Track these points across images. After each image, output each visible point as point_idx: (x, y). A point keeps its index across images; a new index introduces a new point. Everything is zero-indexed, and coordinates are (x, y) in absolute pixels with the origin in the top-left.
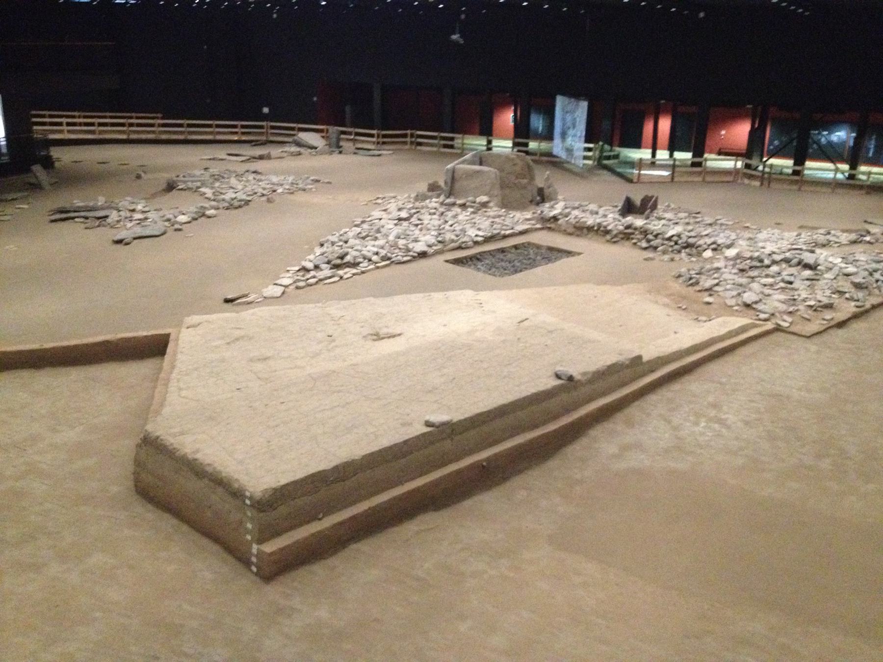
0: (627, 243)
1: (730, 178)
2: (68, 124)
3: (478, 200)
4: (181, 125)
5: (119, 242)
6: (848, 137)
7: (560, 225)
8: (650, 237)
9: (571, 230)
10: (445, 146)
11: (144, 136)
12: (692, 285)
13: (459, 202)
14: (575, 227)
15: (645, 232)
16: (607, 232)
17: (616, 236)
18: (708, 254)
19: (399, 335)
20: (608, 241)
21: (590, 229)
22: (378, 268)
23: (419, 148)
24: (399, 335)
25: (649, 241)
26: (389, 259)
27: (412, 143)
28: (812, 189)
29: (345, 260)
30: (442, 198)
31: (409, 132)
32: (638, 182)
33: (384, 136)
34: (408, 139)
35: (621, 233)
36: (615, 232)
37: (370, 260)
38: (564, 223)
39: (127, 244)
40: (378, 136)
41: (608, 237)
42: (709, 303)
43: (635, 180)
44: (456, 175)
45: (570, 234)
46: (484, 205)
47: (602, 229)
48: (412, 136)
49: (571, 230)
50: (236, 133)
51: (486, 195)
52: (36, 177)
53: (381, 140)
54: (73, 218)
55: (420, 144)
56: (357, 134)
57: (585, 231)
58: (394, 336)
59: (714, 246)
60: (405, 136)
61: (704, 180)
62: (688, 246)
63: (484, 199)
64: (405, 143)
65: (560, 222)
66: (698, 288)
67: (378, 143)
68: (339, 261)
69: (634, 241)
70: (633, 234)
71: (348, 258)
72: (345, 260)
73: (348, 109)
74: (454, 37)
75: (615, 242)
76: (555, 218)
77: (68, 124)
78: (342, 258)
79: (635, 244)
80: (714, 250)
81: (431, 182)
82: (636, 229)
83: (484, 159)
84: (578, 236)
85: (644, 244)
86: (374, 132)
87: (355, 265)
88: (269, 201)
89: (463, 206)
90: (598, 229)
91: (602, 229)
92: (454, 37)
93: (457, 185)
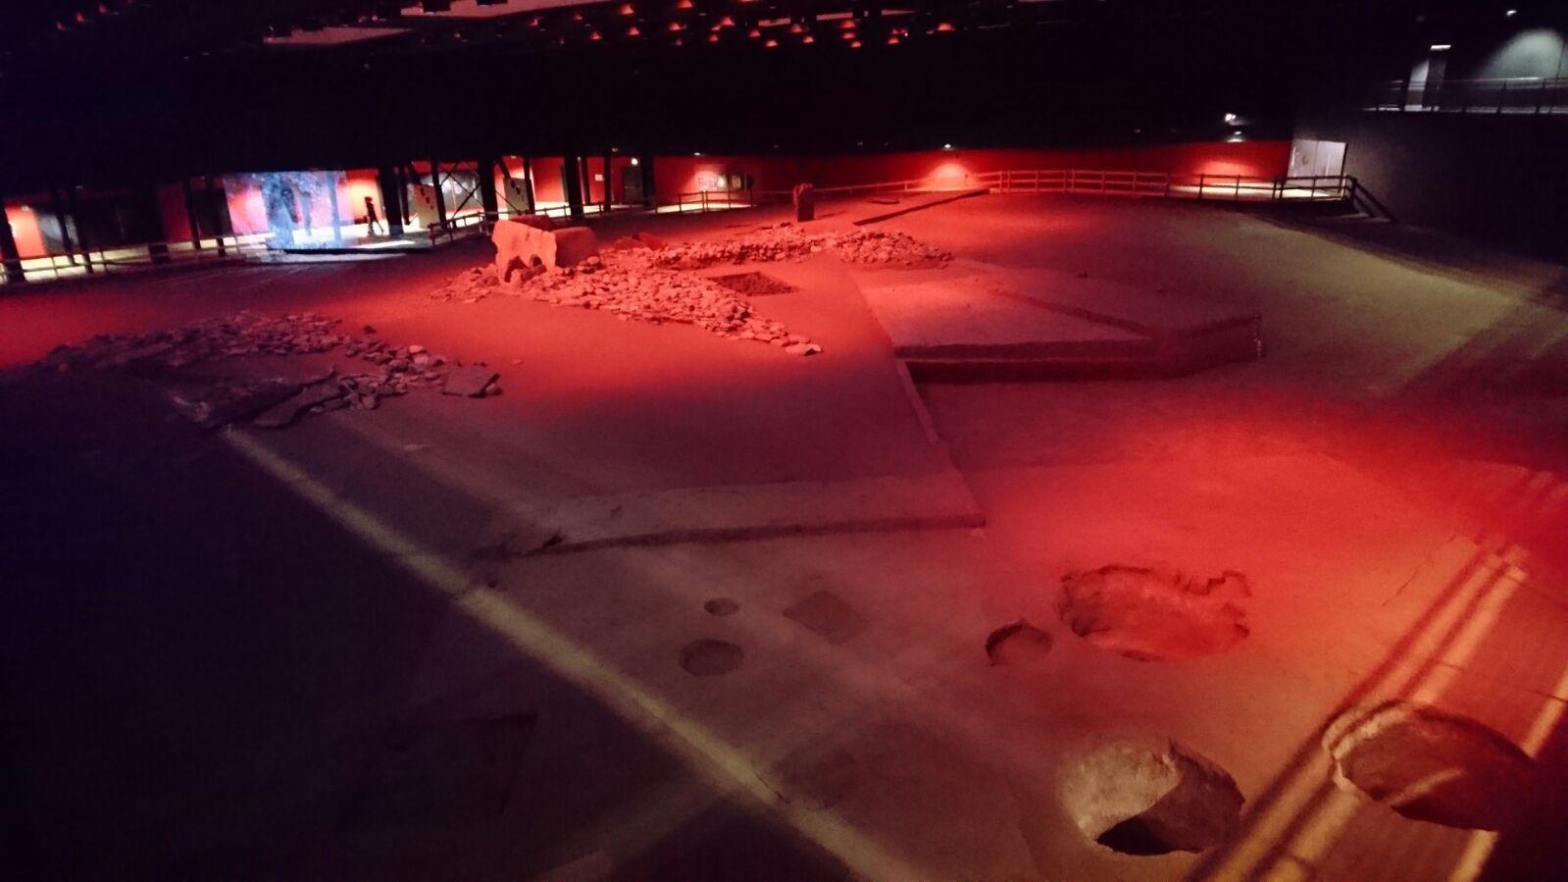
7: (685, 263)
9: (697, 264)
14: (700, 260)
15: (758, 248)
18: (814, 249)
21: (714, 258)
38: (689, 260)
45: (698, 268)
47: (726, 254)
49: (697, 264)
62: (791, 248)
65: (683, 259)
69: (753, 257)
70: (747, 252)
76: (677, 259)
79: (754, 260)
84: (704, 267)
85: (765, 258)
90: (722, 256)
91: (726, 254)
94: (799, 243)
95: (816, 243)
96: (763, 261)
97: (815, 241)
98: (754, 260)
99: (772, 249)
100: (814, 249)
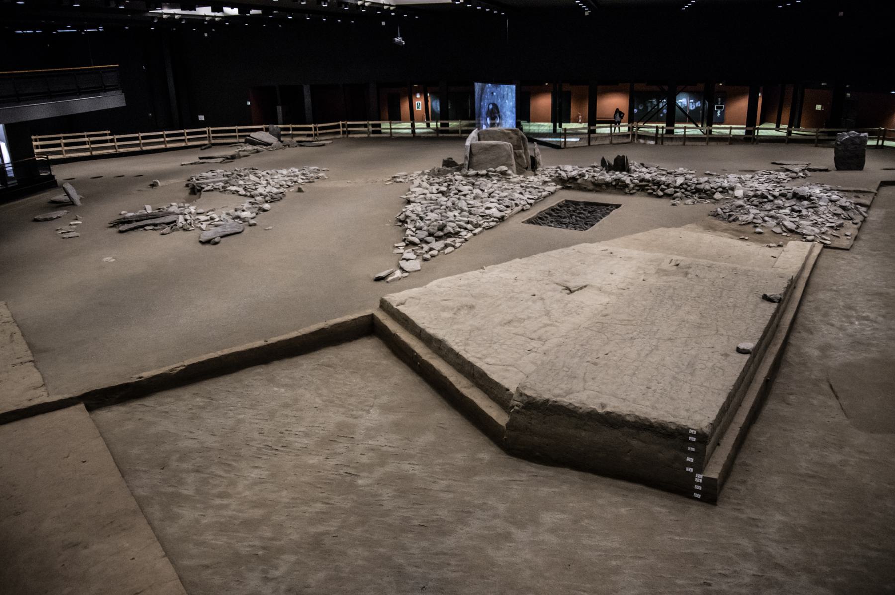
0: (643, 193)
1: (629, 140)
2: (66, 145)
3: (498, 169)
4: (137, 138)
5: (208, 242)
6: (688, 103)
8: (663, 186)
10: (374, 132)
11: (105, 152)
12: (734, 220)
13: (484, 172)
14: (593, 184)
15: (658, 184)
16: (627, 186)
17: (633, 189)
18: (718, 196)
19: (585, 286)
20: (626, 194)
21: (607, 184)
22: (475, 234)
23: (350, 136)
24: (585, 286)
25: (663, 190)
26: (480, 226)
27: (344, 132)
28: (693, 143)
29: (445, 231)
30: (465, 171)
31: (340, 123)
32: (565, 147)
33: (320, 129)
34: (341, 130)
35: (637, 185)
36: (632, 186)
37: (466, 229)
39: (216, 243)
40: (315, 130)
41: (627, 190)
42: (760, 233)
43: (563, 146)
44: (474, 151)
45: (590, 191)
46: (504, 173)
48: (343, 126)
49: (591, 187)
50: (235, 136)
51: (503, 164)
52: (68, 195)
53: (318, 132)
54: (143, 227)
55: (349, 132)
56: (294, 129)
57: (604, 187)
58: (581, 288)
59: (721, 190)
60: (338, 126)
61: (611, 143)
62: (698, 191)
63: (504, 168)
64: (338, 133)
65: (579, 181)
66: (738, 222)
67: (316, 135)
68: (441, 233)
71: (449, 228)
72: (445, 231)
73: (280, 109)
74: (398, 39)
75: (632, 194)
76: (574, 179)
77: (66, 145)
78: (441, 229)
80: (721, 192)
81: (445, 158)
82: (649, 181)
83: (482, 136)
84: (597, 192)
85: (661, 194)
86: (312, 126)
87: (457, 234)
88: (300, 190)
89: (487, 176)
90: (617, 184)
92: (398, 39)
93: (475, 159)
94: (707, 187)
95: (724, 191)
96: (658, 197)
97: (724, 189)
98: (650, 194)
99: (675, 187)
100: (718, 196)
